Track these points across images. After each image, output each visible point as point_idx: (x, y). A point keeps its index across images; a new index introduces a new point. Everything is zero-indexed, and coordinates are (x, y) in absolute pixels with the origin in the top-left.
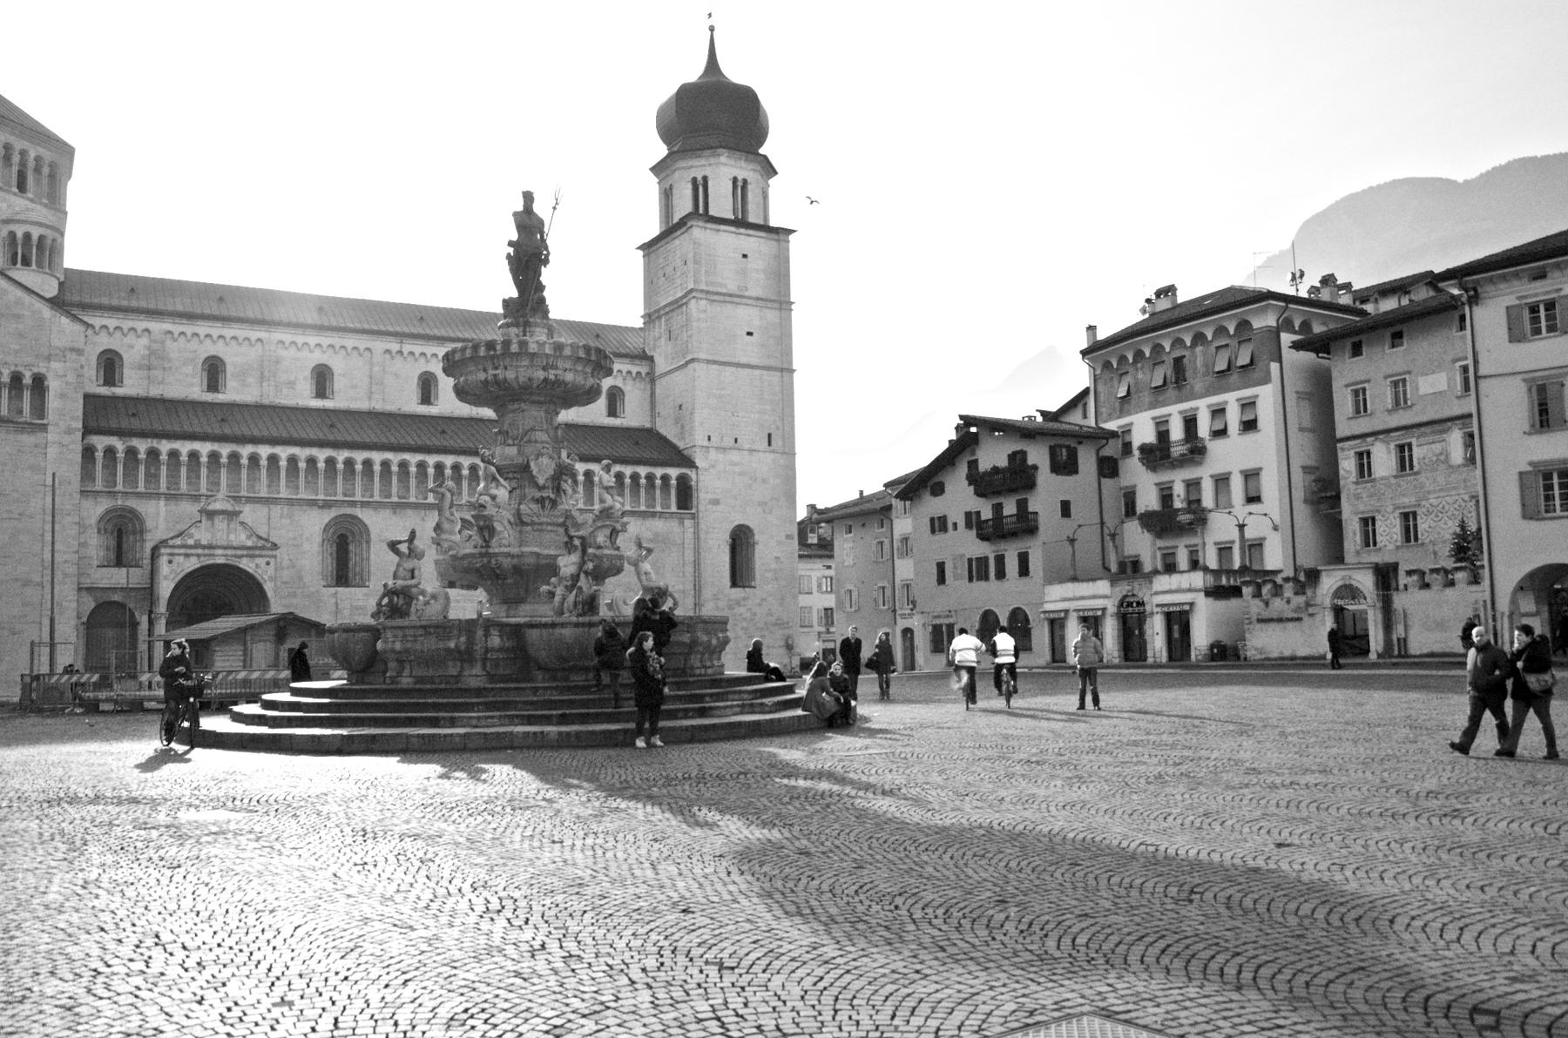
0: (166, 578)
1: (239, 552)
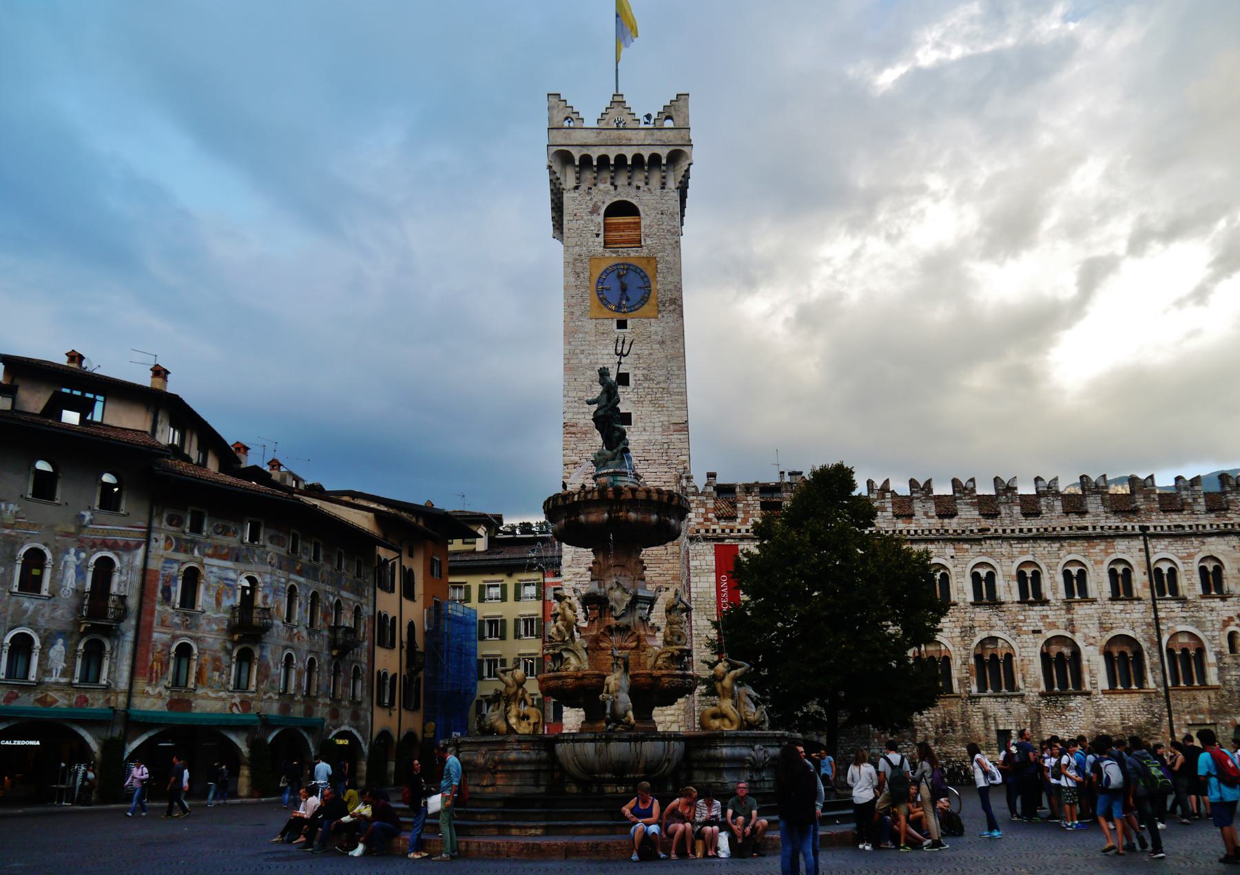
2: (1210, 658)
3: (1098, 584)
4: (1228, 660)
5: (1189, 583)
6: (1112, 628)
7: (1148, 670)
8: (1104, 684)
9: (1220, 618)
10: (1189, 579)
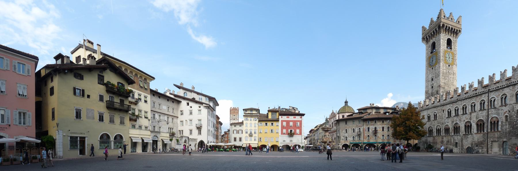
2: (500, 123)
3: (478, 107)
6: (478, 118)
7: (485, 128)
8: (475, 131)
9: (504, 112)
10: (498, 102)
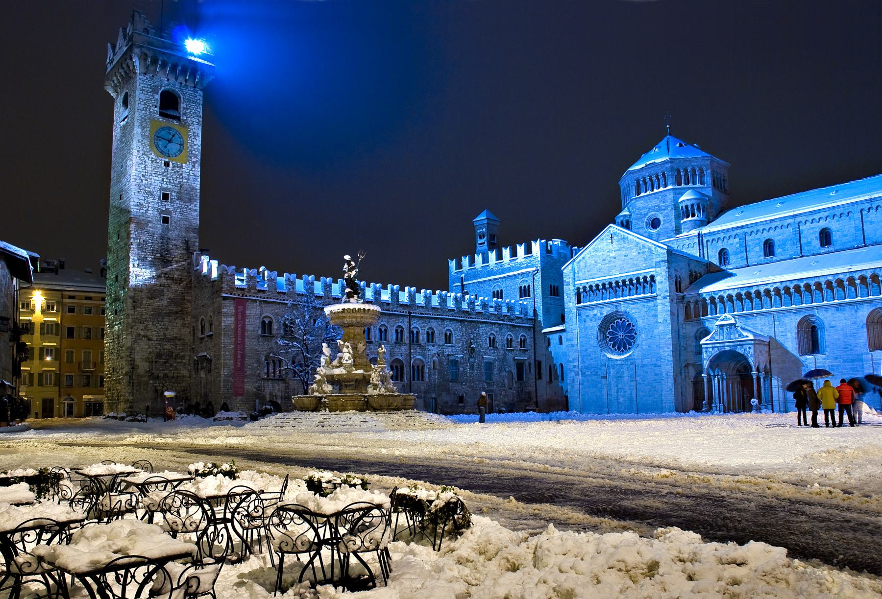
0: (705, 359)
1: (736, 343)
2: (427, 370)
3: (392, 336)
4: (432, 371)
5: (423, 338)
